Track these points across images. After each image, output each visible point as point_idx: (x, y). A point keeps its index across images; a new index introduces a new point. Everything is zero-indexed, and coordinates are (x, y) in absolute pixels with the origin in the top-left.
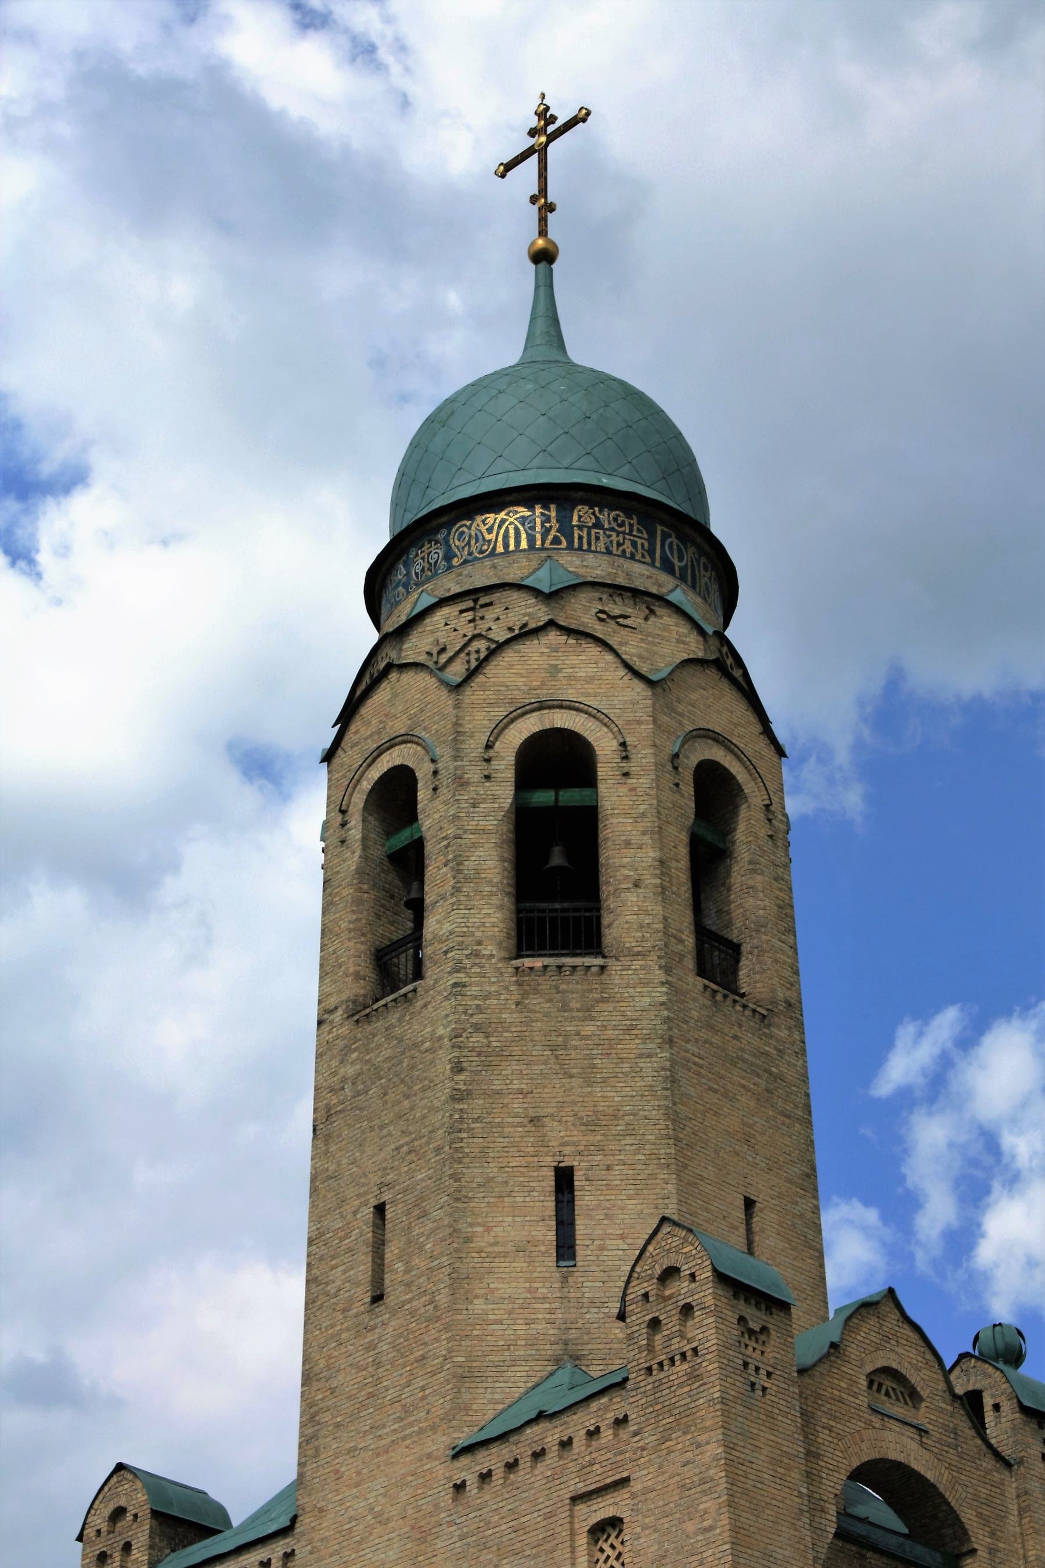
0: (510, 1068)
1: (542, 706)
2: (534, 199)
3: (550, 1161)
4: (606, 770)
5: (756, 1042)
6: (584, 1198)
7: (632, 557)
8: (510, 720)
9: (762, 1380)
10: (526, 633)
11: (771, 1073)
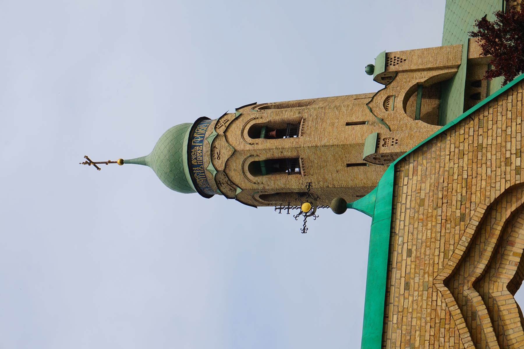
0: (327, 177)
1: (244, 172)
2: (107, 164)
3: (346, 168)
4: (257, 159)
5: (310, 122)
6: (353, 161)
7: (202, 150)
8: (248, 179)
9: (394, 140)
10: (227, 175)
11: (316, 118)
